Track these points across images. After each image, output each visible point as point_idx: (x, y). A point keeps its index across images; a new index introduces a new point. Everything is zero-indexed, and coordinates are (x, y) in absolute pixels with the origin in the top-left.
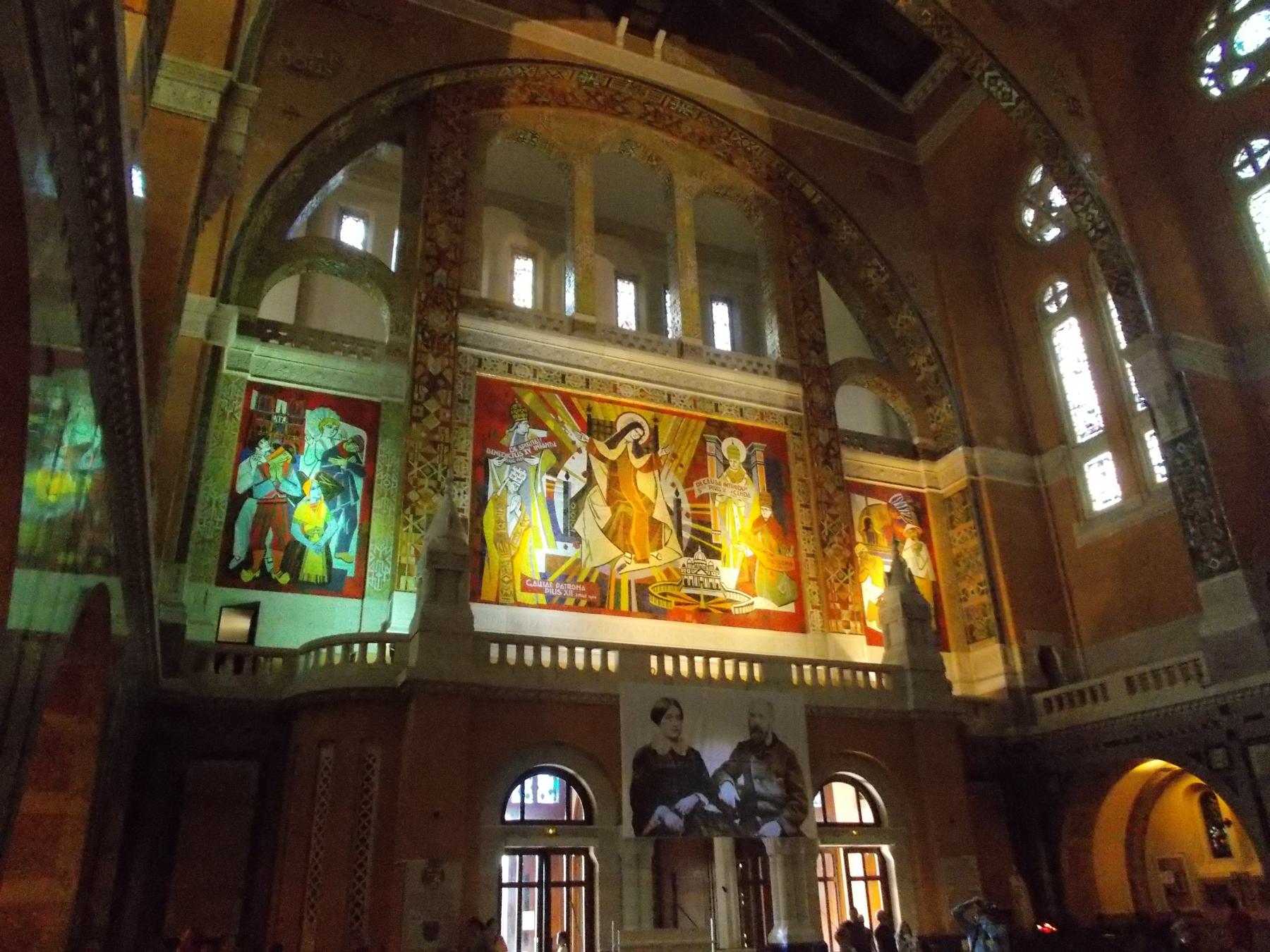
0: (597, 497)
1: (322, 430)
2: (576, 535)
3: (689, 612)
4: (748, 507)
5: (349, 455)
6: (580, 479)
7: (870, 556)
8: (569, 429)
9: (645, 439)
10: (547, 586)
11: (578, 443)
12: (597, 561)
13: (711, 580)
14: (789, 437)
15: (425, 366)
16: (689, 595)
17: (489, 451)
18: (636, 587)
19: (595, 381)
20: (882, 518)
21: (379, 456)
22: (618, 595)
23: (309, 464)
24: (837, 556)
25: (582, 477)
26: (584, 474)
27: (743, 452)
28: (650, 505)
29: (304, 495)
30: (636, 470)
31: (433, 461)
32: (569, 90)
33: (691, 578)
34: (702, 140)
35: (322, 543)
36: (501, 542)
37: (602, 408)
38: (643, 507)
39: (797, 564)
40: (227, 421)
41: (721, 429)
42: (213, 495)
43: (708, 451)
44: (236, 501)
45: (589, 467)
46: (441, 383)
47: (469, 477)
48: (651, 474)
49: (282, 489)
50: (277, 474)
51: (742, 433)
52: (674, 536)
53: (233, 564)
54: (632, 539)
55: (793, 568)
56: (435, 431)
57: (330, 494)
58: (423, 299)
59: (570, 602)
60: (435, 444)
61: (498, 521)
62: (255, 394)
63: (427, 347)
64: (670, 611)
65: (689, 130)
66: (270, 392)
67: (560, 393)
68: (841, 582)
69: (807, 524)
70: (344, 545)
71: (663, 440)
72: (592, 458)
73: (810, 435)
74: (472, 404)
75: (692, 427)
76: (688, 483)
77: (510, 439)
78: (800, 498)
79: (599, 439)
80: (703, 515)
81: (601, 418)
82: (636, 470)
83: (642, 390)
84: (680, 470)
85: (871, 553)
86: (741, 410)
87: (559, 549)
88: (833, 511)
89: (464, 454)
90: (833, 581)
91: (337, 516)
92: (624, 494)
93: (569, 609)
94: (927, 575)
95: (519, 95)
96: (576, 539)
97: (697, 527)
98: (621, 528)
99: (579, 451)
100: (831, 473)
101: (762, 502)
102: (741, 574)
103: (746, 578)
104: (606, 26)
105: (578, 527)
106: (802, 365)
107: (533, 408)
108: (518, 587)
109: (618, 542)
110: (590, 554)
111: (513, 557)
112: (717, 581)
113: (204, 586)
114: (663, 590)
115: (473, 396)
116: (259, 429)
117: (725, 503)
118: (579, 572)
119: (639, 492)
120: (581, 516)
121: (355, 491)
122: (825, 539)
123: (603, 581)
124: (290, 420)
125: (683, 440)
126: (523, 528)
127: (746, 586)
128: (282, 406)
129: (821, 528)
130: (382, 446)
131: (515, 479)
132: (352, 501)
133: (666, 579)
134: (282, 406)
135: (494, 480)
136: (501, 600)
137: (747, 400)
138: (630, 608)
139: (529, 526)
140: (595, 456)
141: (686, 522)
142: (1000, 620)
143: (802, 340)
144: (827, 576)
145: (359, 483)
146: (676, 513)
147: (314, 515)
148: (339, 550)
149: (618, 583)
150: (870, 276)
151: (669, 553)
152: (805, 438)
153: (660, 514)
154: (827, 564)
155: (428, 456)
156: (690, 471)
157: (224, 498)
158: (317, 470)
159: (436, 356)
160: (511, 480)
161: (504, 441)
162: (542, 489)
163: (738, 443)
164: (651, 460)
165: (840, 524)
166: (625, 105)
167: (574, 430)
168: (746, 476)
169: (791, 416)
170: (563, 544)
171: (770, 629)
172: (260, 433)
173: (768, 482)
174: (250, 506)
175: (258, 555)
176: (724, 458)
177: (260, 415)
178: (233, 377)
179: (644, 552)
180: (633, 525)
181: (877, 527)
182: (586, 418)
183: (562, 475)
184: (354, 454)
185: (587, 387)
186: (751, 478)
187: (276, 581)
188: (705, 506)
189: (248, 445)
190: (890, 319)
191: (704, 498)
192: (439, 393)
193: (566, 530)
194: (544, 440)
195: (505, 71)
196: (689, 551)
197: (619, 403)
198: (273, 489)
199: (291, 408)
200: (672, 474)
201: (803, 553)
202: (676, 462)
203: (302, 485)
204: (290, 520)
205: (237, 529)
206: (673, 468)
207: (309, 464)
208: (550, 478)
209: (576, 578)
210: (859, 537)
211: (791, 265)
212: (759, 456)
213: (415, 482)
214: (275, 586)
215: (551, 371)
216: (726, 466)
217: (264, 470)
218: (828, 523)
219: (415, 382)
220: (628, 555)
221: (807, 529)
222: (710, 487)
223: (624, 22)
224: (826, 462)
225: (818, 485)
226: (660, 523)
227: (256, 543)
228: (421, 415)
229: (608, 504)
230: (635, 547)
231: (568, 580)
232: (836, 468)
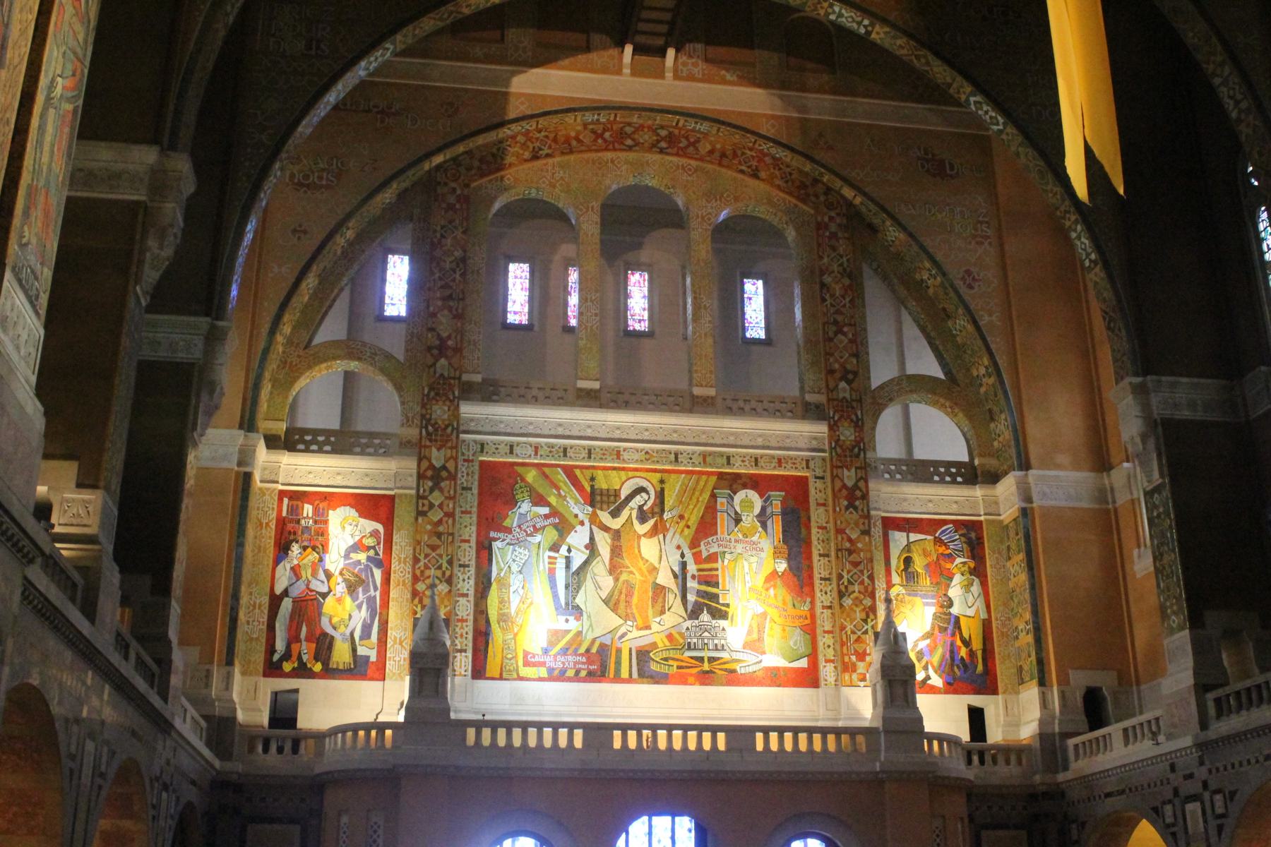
0: (599, 568)
1: (344, 528)
2: (578, 608)
3: (691, 675)
4: (760, 564)
5: (368, 548)
6: (583, 552)
7: (907, 598)
8: (572, 502)
9: (650, 503)
10: (548, 660)
11: (581, 517)
12: (598, 633)
13: (716, 641)
14: (811, 481)
15: (429, 460)
16: (692, 658)
17: (493, 534)
18: (637, 655)
19: (597, 450)
20: (926, 554)
21: (394, 548)
22: (618, 663)
24: (857, 606)
25: (584, 550)
26: (586, 547)
27: (758, 503)
28: (654, 570)
29: (330, 591)
30: (639, 537)
31: (438, 552)
32: (573, 134)
33: (695, 640)
34: (723, 155)
35: (348, 633)
36: (504, 621)
37: (605, 477)
38: (646, 573)
39: (813, 617)
40: (264, 531)
41: (734, 482)
42: (253, 603)
43: (719, 507)
44: (275, 601)
45: (592, 538)
46: (444, 474)
47: (473, 563)
48: (655, 540)
49: (312, 586)
50: (306, 573)
52: (679, 599)
53: (276, 657)
54: (634, 607)
55: (808, 622)
56: (440, 522)
57: (352, 589)
58: (426, 392)
59: (570, 673)
60: (439, 535)
61: (502, 602)
62: (286, 501)
63: (431, 440)
64: (672, 675)
65: (709, 147)
66: (297, 497)
67: (565, 468)
68: (859, 633)
69: (825, 574)
70: (366, 634)
72: (595, 529)
73: (833, 478)
74: (475, 491)
75: (702, 483)
76: (694, 544)
77: (512, 520)
78: (819, 547)
79: (601, 509)
80: (712, 576)
81: (604, 486)
82: (639, 537)
83: (647, 453)
84: (687, 531)
85: (909, 595)
86: (756, 459)
87: (560, 623)
88: (854, 557)
89: (468, 541)
90: (849, 633)
91: (359, 607)
92: (627, 562)
93: (570, 680)
94: (978, 611)
95: (521, 152)
96: (577, 611)
97: (703, 588)
98: (623, 596)
99: (582, 523)
100: (855, 516)
101: (777, 554)
102: (750, 632)
103: (755, 636)
104: (614, 52)
105: (579, 600)
106: (829, 400)
107: (536, 486)
108: (521, 663)
109: (619, 611)
110: (591, 625)
111: (516, 635)
112: (723, 642)
113: (253, 679)
114: (665, 655)
115: (476, 483)
116: (290, 533)
117: (735, 560)
118: (580, 645)
119: (642, 558)
120: (583, 588)
121: (374, 582)
122: (844, 590)
124: (316, 522)
125: (691, 499)
126: (525, 606)
127: (755, 645)
129: (840, 577)
130: (396, 538)
131: (518, 559)
132: (372, 593)
133: (667, 643)
134: (308, 509)
135: (498, 562)
136: (505, 676)
137: (764, 447)
138: (630, 674)
139: (532, 603)
140: (599, 527)
141: (692, 584)
142: (1041, 663)
143: (831, 372)
144: (843, 628)
145: (378, 574)
146: (681, 576)
147: (340, 608)
148: (361, 638)
149: (619, 651)
150: (925, 277)
151: (674, 617)
152: (828, 479)
153: (665, 579)
154: (845, 615)
155: (434, 548)
156: (697, 531)
157: (265, 600)
158: (341, 566)
159: (439, 449)
160: (514, 561)
161: (507, 523)
162: (544, 565)
164: (655, 525)
165: (862, 572)
166: (636, 136)
167: (577, 502)
168: (760, 529)
169: (813, 458)
170: (564, 618)
171: (779, 686)
172: (292, 537)
173: (784, 531)
174: (287, 604)
175: (294, 647)
176: (736, 513)
177: (291, 521)
178: (268, 489)
179: (646, 618)
180: (636, 593)
181: (919, 564)
182: (589, 489)
183: (564, 550)
184: (374, 548)
185: (590, 457)
186: (766, 531)
187: (311, 669)
188: (714, 565)
189: (283, 549)
190: (950, 323)
191: (713, 558)
192: (443, 484)
193: (567, 604)
194: (547, 517)
195: (506, 132)
196: (694, 614)
197: (623, 469)
198: (304, 587)
199: (316, 510)
200: (677, 536)
201: (818, 605)
202: (683, 524)
203: (328, 581)
204: (320, 614)
205: (277, 625)
206: (679, 530)
208: (552, 554)
209: (576, 650)
210: (896, 579)
211: (823, 285)
212: (777, 506)
213: (422, 572)
214: (311, 675)
215: (551, 446)
216: (738, 520)
217: (296, 571)
218: (849, 572)
219: (420, 476)
220: (629, 623)
221: (825, 579)
222: (719, 546)
223: (629, 49)
224: (851, 505)
225: (840, 531)
226: (664, 588)
228: (426, 508)
229: (611, 574)
230: (637, 616)
231: (570, 651)
232: (863, 510)
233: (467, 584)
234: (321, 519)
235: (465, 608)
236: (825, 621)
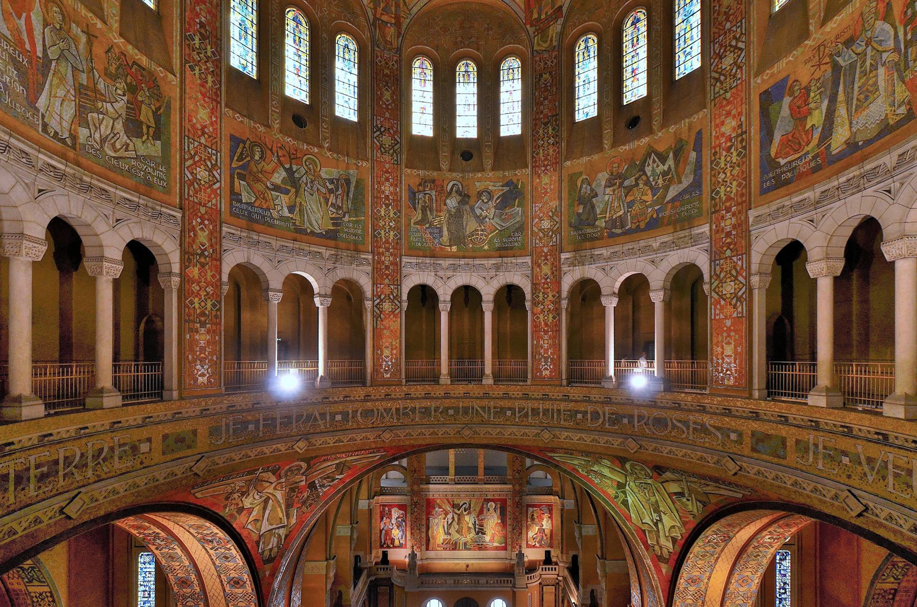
0: (455, 523)
23: (394, 521)
41: (488, 501)
44: (381, 531)
50: (387, 524)
51: (493, 500)
70: (402, 537)
71: (472, 506)
76: (478, 517)
77: (434, 512)
87: (446, 537)
105: (450, 531)
123: (456, 543)
127: (492, 540)
128: (387, 509)
134: (387, 509)
146: (474, 524)
153: (471, 525)
163: (493, 503)
174: (384, 531)
189: (382, 519)
191: (482, 520)
196: (477, 534)
207: (394, 521)
212: (499, 506)
214: (390, 548)
227: (386, 539)
233: (424, 530)
234: (390, 511)
235: (424, 535)
236: (509, 536)
